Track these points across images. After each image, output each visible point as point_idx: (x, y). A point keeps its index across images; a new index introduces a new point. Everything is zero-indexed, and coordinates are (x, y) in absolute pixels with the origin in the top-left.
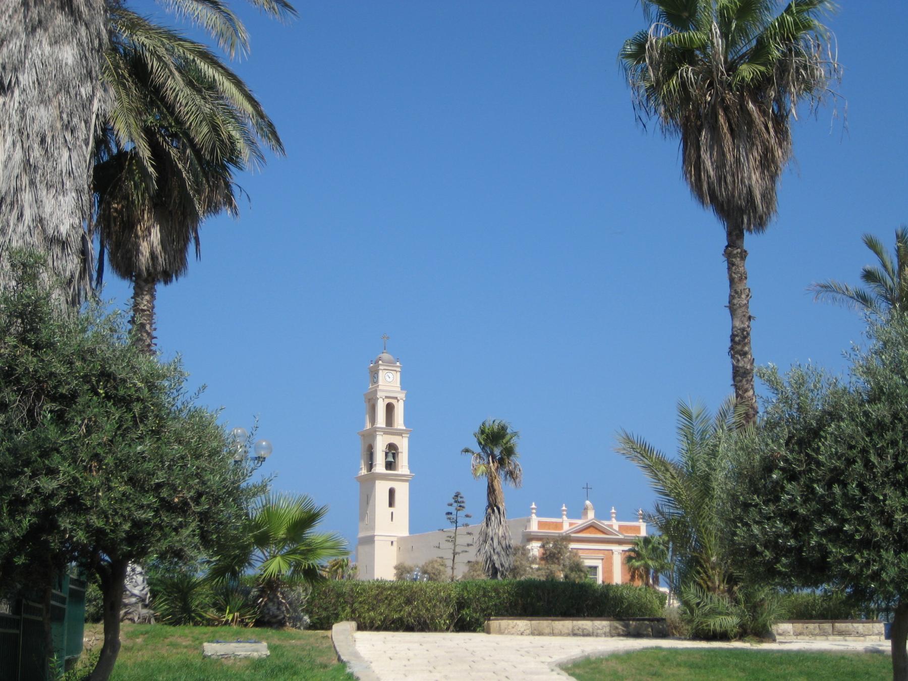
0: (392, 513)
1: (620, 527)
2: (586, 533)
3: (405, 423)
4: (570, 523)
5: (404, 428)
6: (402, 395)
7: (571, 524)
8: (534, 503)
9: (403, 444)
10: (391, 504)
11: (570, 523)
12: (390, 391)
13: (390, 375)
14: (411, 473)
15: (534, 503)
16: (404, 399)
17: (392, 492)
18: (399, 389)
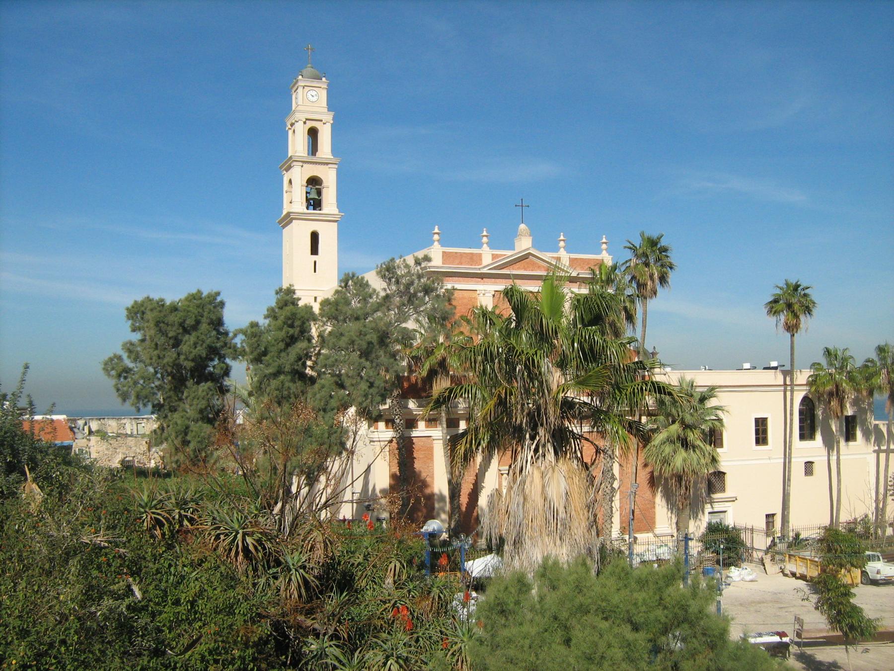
0: (315, 263)
1: (572, 261)
2: (519, 269)
3: (334, 151)
4: (493, 255)
5: (332, 157)
6: (329, 117)
7: (494, 257)
8: (437, 227)
9: (329, 178)
10: (314, 250)
11: (493, 255)
12: (313, 112)
13: (314, 93)
14: (339, 212)
15: (437, 227)
16: (332, 122)
17: (315, 237)
18: (326, 110)
